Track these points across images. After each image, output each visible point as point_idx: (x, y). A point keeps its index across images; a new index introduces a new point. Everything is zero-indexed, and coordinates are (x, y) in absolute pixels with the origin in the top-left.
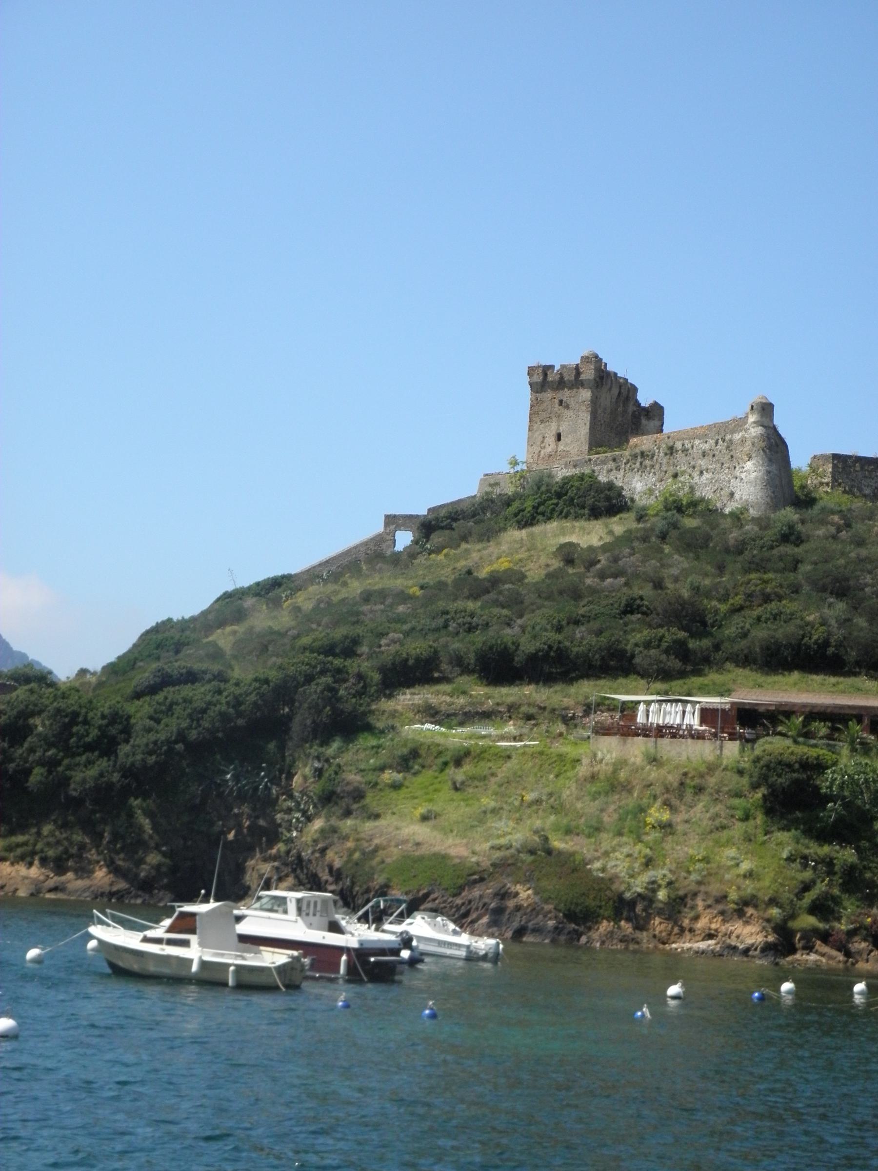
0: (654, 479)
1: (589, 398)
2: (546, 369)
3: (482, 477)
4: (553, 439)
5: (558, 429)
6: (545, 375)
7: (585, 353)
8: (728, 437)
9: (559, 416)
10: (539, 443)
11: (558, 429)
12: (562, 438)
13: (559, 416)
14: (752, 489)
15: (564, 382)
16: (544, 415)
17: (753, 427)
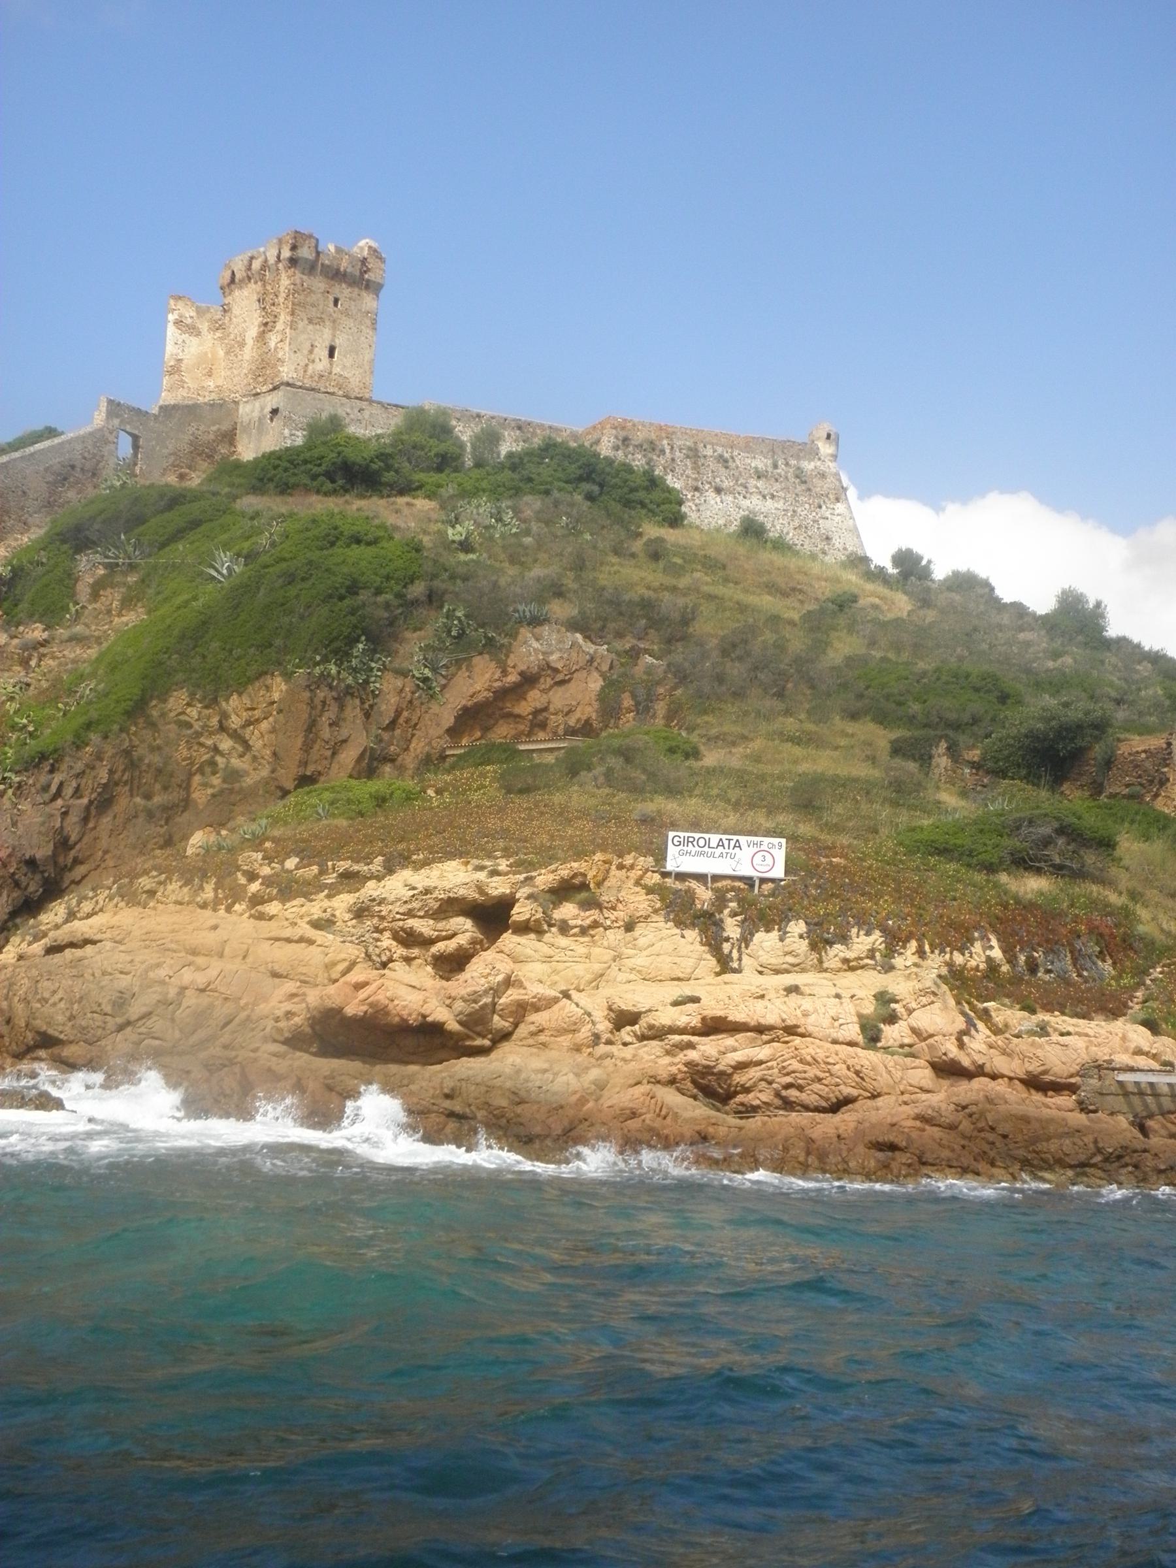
4: (327, 352)
5: (333, 340)
8: (793, 462)
9: (334, 321)
10: (306, 352)
11: (333, 340)
16: (313, 312)
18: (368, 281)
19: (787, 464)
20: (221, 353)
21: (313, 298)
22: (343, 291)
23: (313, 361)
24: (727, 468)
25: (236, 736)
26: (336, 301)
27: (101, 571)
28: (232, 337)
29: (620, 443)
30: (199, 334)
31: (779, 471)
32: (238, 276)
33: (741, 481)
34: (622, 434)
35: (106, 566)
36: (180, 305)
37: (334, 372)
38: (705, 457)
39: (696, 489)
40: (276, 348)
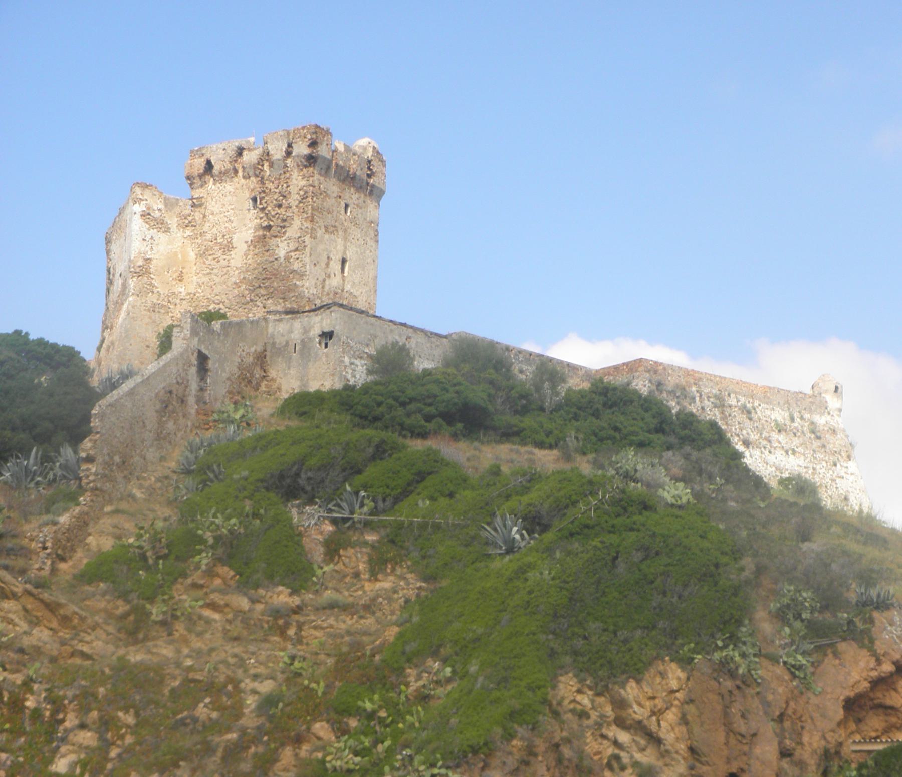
5: (345, 253)
8: (807, 416)
9: (345, 231)
10: (323, 265)
16: (329, 220)
18: (373, 186)
19: (802, 418)
20: (192, 255)
21: (330, 202)
22: (352, 196)
23: (329, 276)
24: (750, 419)
25: (639, 728)
27: (329, 528)
28: (209, 237)
30: (167, 230)
31: (796, 425)
32: (217, 169)
33: (765, 434)
35: (334, 521)
36: (147, 194)
40: (287, 258)
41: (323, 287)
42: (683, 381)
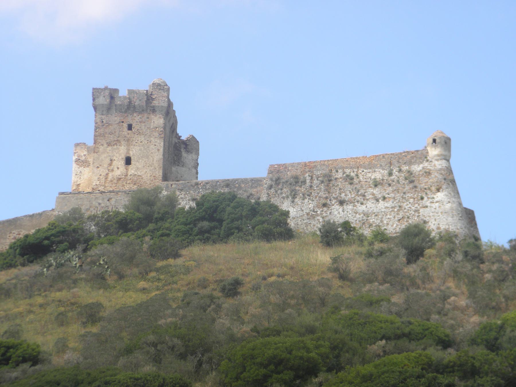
0: (311, 206)
1: (162, 125)
2: (113, 94)
3: (58, 196)
4: (123, 162)
6: (112, 98)
7: (157, 81)
9: (128, 140)
10: (106, 166)
11: (128, 153)
12: (132, 162)
13: (128, 141)
14: (450, 219)
15: (134, 107)
16: (112, 138)
17: (437, 160)
19: (400, 171)
22: (135, 119)
23: (113, 170)
24: (351, 184)
26: (130, 127)
29: (273, 183)
31: (392, 177)
33: (362, 191)
34: (276, 176)
37: (129, 173)
38: (336, 179)
39: (325, 205)
41: (106, 179)
42: (299, 173)
